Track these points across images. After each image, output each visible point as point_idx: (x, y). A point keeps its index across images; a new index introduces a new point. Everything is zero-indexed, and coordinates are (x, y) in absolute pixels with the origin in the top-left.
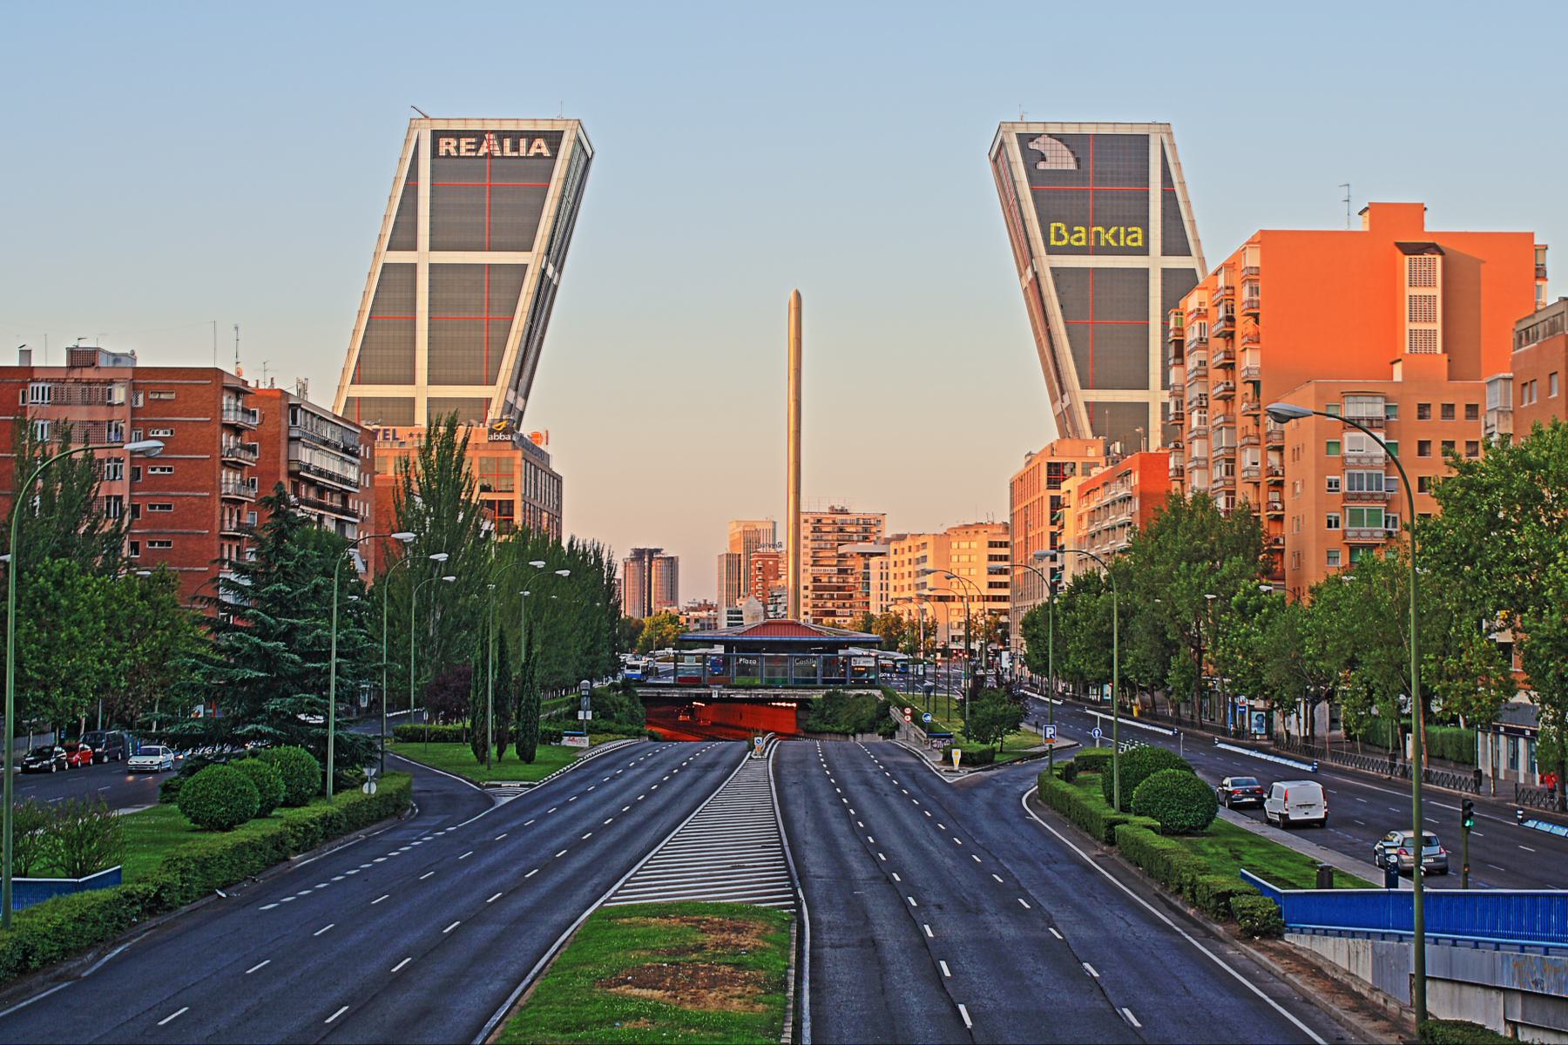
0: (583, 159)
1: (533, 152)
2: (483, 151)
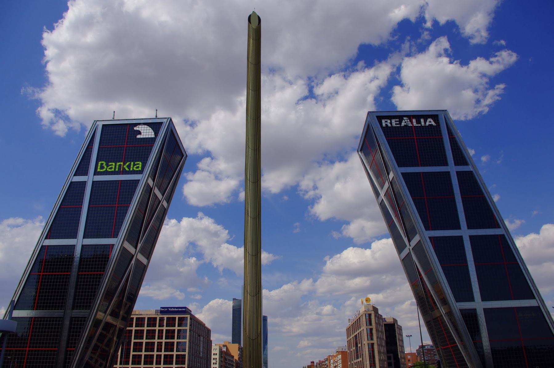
1: (427, 124)
2: (403, 124)
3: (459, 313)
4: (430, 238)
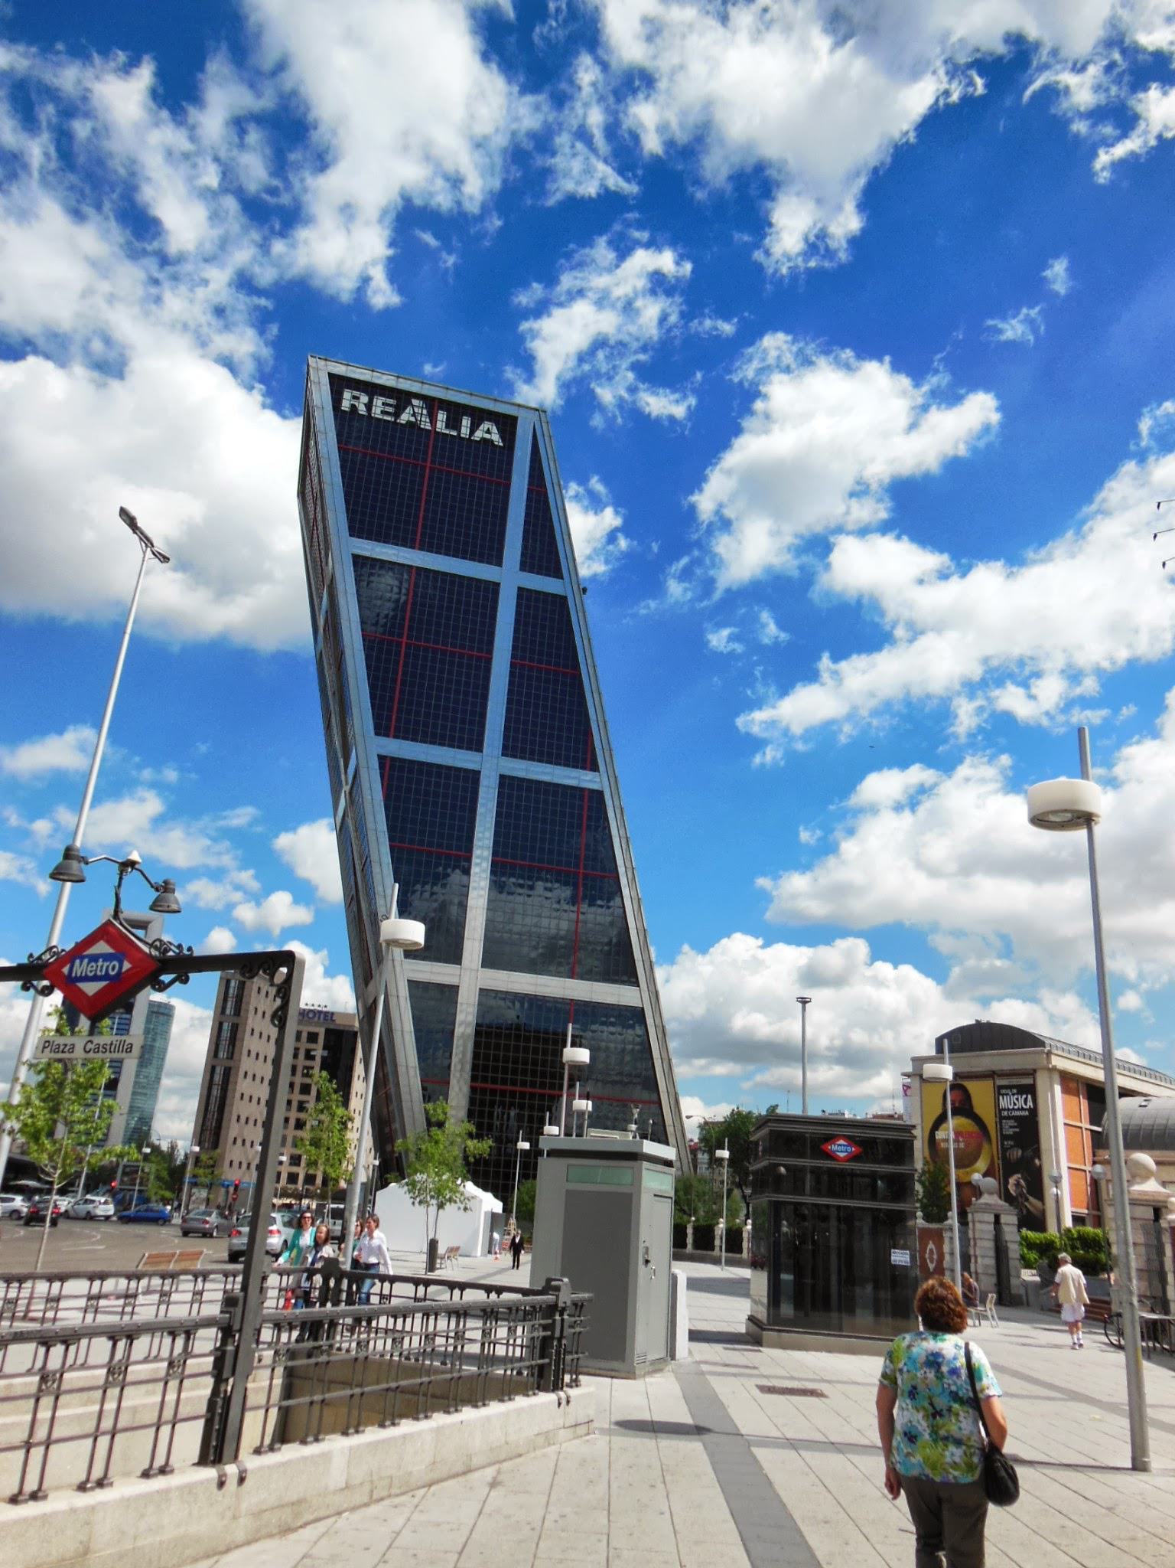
1: (479, 435)
2: (405, 417)
3: (404, 991)
4: (382, 759)
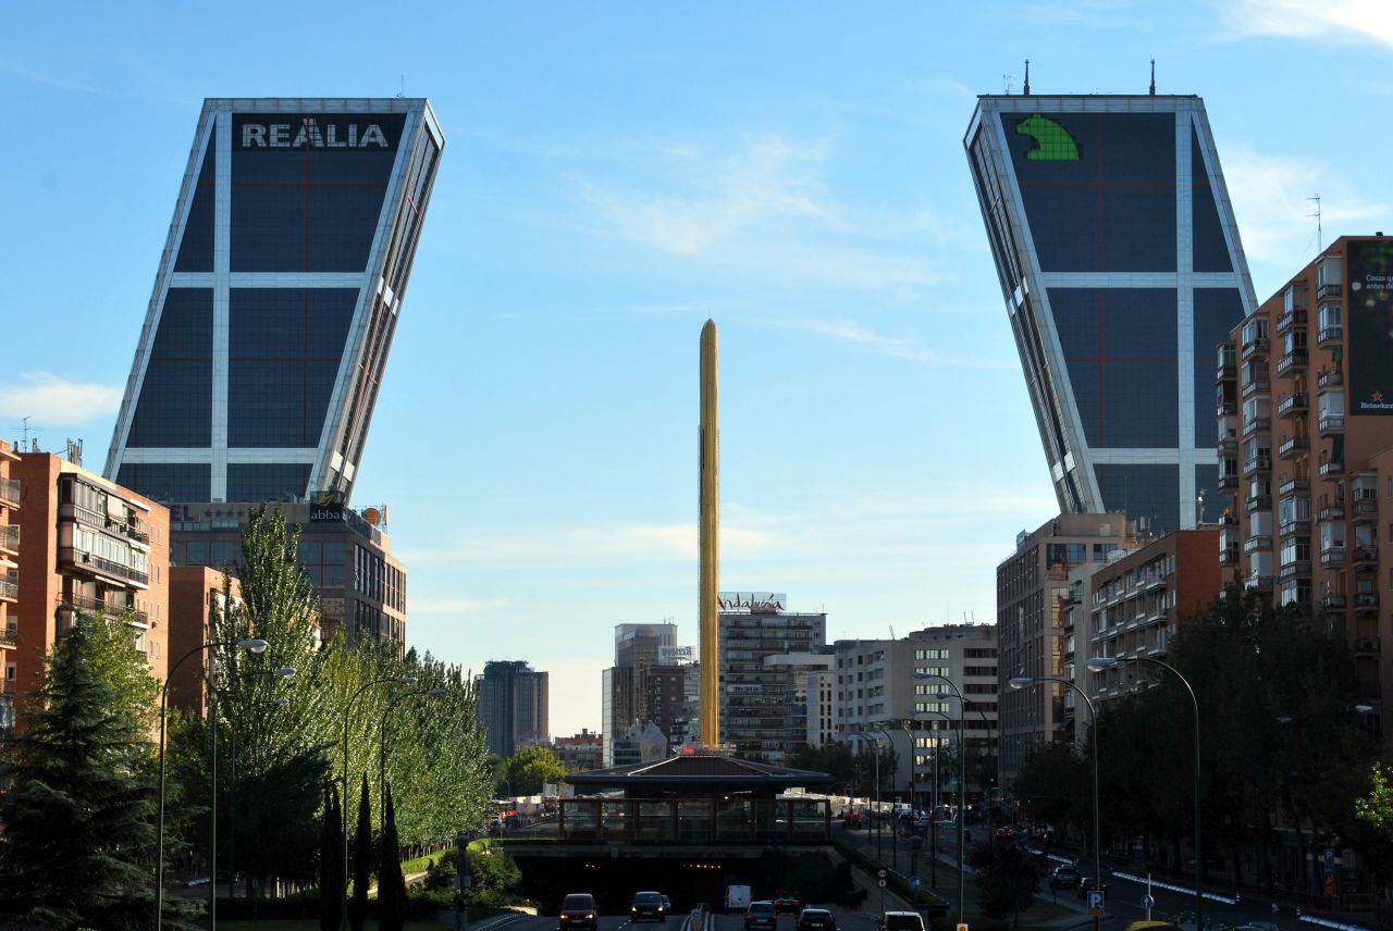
0: (431, 149)
1: (365, 140)
2: (300, 139)
